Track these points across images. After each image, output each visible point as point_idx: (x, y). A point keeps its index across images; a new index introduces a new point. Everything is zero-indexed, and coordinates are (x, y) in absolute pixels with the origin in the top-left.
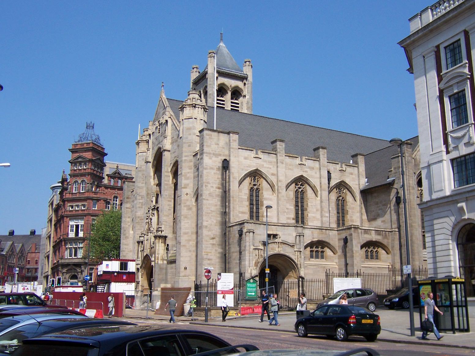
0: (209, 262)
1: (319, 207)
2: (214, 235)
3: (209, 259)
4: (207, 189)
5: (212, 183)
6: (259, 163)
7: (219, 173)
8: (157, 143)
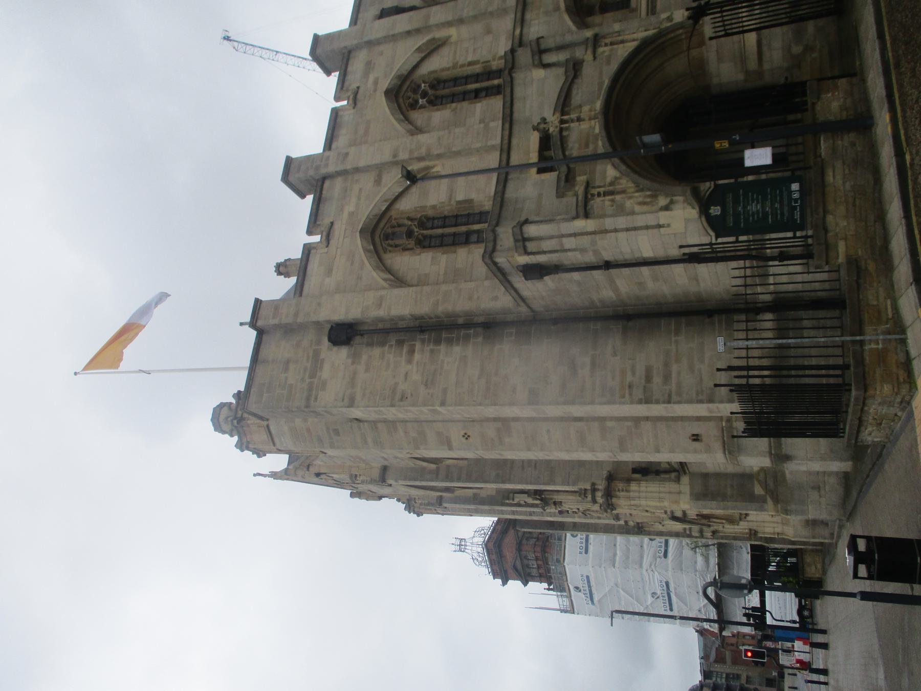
0: (657, 380)
1: (478, 27)
3: (649, 379)
4: (412, 395)
5: (394, 377)
6: (344, 227)
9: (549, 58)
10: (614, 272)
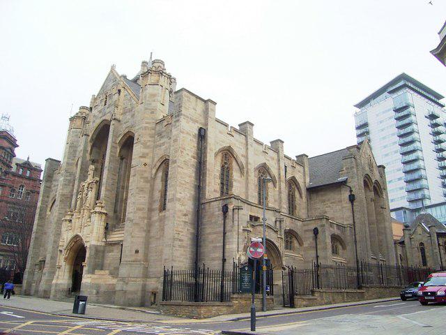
1: (277, 197)
2: (187, 211)
7: (195, 140)
8: (101, 115)
9: (278, 223)
10: (222, 234)
